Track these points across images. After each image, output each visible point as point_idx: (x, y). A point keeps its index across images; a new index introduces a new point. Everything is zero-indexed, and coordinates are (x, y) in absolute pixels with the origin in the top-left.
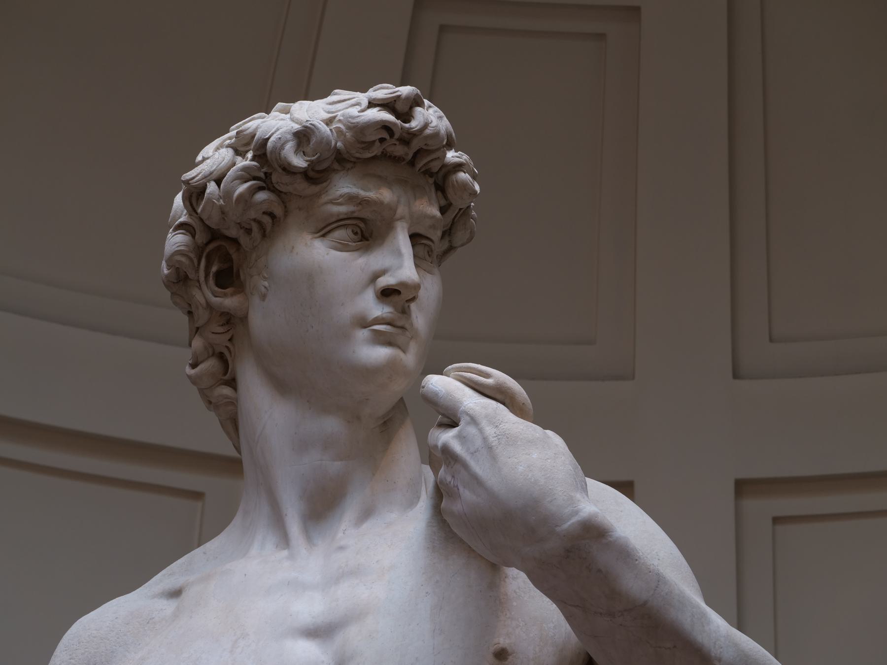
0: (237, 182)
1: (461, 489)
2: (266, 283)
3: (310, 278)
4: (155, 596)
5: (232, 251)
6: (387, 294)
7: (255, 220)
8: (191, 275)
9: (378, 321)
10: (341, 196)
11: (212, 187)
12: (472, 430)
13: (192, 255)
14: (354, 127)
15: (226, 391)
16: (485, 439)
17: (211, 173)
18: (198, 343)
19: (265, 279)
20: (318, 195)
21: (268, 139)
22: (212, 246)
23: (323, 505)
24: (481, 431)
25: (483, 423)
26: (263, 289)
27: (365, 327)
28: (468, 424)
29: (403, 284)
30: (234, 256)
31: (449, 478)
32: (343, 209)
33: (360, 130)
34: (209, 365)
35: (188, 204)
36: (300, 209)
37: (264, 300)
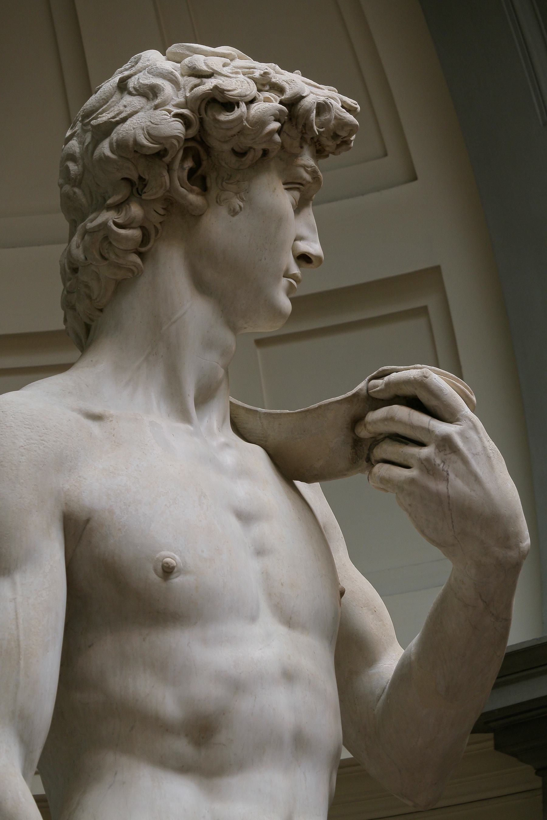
0: (273, 118)
1: (452, 476)
2: (241, 204)
3: (279, 221)
4: (73, 410)
5: (203, 156)
6: (304, 258)
7: (254, 149)
8: (167, 159)
9: (294, 277)
10: (311, 167)
11: (243, 107)
12: (472, 434)
13: (182, 144)
14: (340, 119)
15: (139, 261)
16: (484, 448)
17: (246, 96)
18: (135, 210)
19: (242, 200)
20: (296, 156)
21: (303, 97)
22: (190, 144)
23: (204, 398)
24: (480, 438)
25: (482, 435)
26: (238, 208)
27: (284, 277)
28: (471, 428)
29: (319, 258)
30: (204, 163)
31: (438, 461)
32: (307, 177)
33: (342, 123)
34: (135, 233)
35: (199, 102)
36: (281, 159)
37: (233, 216)
